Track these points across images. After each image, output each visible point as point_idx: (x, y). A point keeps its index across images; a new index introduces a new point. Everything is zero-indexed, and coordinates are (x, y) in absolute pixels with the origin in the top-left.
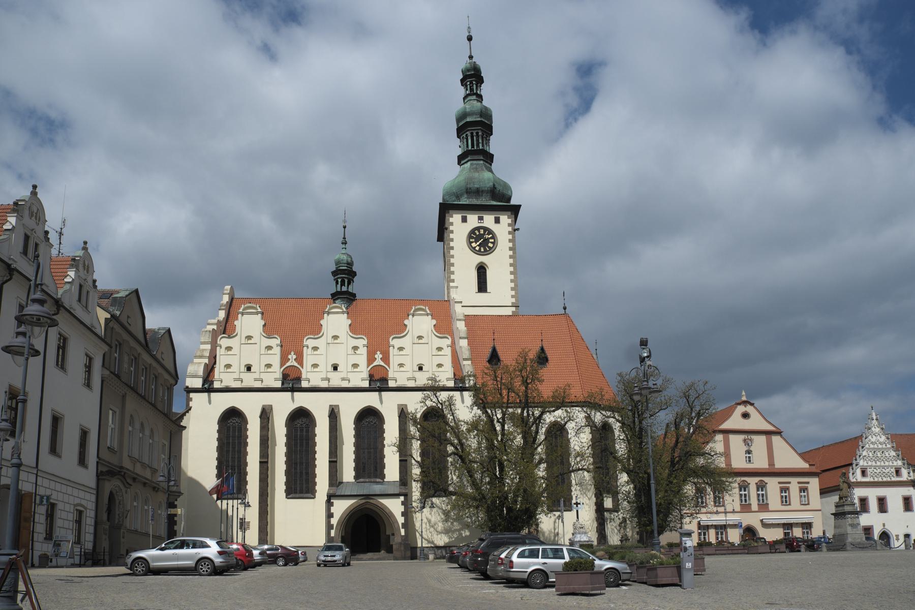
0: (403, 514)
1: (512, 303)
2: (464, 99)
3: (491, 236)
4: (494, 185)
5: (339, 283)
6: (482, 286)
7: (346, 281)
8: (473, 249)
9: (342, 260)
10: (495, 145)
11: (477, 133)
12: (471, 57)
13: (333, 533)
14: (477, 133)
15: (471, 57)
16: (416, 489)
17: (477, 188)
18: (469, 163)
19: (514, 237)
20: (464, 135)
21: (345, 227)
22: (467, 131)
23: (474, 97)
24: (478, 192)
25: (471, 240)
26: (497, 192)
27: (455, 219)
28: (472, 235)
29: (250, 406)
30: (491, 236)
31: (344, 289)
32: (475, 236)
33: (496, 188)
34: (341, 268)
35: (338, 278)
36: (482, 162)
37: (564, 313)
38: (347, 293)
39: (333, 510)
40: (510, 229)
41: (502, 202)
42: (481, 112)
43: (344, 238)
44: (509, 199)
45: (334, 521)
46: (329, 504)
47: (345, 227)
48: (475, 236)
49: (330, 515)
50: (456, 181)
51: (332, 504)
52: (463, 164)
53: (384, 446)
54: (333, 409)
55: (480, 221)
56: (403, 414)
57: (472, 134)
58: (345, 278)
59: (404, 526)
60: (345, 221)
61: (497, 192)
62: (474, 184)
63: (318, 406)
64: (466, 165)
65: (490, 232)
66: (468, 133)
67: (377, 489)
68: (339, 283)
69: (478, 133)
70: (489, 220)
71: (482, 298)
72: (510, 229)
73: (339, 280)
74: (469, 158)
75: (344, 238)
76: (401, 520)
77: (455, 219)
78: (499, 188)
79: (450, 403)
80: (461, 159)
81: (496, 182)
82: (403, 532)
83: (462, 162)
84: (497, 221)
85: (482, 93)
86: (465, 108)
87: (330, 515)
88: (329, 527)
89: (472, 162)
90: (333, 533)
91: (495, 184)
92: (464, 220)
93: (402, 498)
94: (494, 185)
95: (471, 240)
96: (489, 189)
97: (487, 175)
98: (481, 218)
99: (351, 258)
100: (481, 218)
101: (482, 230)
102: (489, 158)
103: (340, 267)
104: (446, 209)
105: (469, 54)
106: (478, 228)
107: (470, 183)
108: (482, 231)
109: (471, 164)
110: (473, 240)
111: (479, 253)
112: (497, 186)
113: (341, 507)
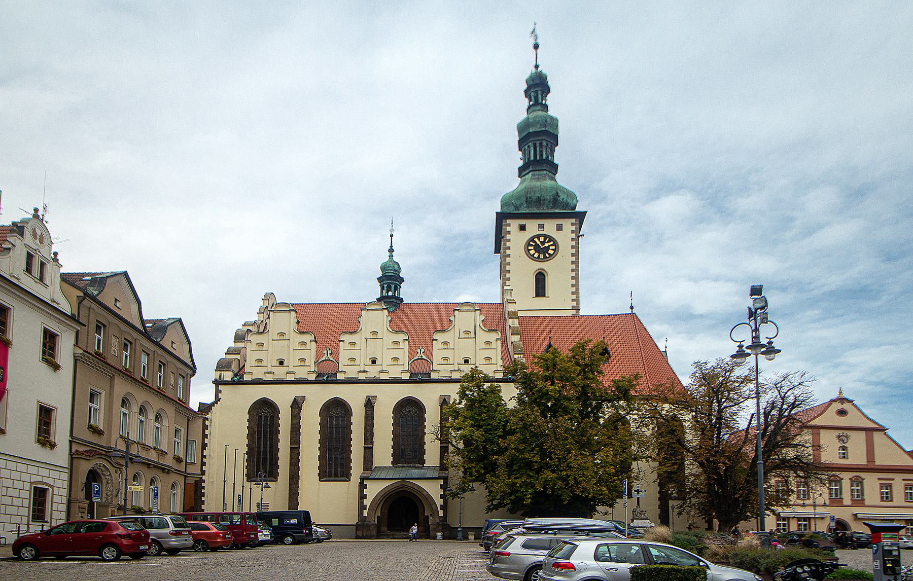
0: (442, 497)
1: (572, 306)
2: (528, 110)
3: (552, 243)
5: (385, 289)
6: (540, 290)
7: (393, 286)
8: (532, 257)
9: (389, 267)
10: (559, 156)
11: (541, 144)
13: (365, 513)
16: (456, 476)
17: (538, 197)
18: (530, 174)
19: (577, 243)
20: (526, 147)
21: (392, 236)
22: (529, 142)
23: (539, 107)
24: (539, 202)
25: (530, 248)
27: (513, 226)
28: (531, 243)
29: (282, 397)
30: (552, 243)
31: (390, 294)
32: (534, 244)
33: (559, 196)
34: (387, 274)
35: (384, 284)
36: (545, 172)
37: (630, 312)
38: (393, 297)
39: (366, 491)
40: (574, 236)
41: (565, 210)
43: (391, 246)
44: (574, 208)
45: (367, 502)
46: (362, 486)
47: (392, 236)
48: (534, 244)
49: (362, 497)
50: (516, 191)
51: (365, 487)
52: (524, 176)
53: (425, 434)
54: (369, 398)
55: (540, 229)
56: (444, 402)
57: (535, 144)
58: (392, 283)
59: (442, 507)
60: (392, 230)
61: (561, 200)
62: (535, 193)
63: (355, 397)
64: (527, 177)
65: (551, 239)
66: (530, 144)
67: (415, 472)
68: (385, 289)
70: (550, 227)
71: (541, 302)
72: (574, 236)
73: (385, 286)
74: (531, 169)
75: (391, 246)
76: (439, 502)
77: (513, 226)
78: (562, 196)
79: (495, 392)
80: (522, 171)
81: (560, 190)
82: (441, 513)
83: (523, 174)
84: (559, 228)
85: (548, 103)
86: (528, 118)
87: (362, 497)
88: (362, 507)
89: (533, 173)
90: (365, 513)
91: (559, 192)
92: (523, 228)
93: (441, 482)
95: (530, 248)
97: (549, 183)
98: (541, 226)
99: (399, 265)
100: (541, 226)
101: (543, 238)
102: (554, 168)
103: (386, 273)
104: (501, 218)
106: (538, 237)
107: (530, 193)
108: (542, 239)
109: (532, 175)
110: (532, 248)
111: (538, 259)
112: (560, 194)
113: (374, 490)
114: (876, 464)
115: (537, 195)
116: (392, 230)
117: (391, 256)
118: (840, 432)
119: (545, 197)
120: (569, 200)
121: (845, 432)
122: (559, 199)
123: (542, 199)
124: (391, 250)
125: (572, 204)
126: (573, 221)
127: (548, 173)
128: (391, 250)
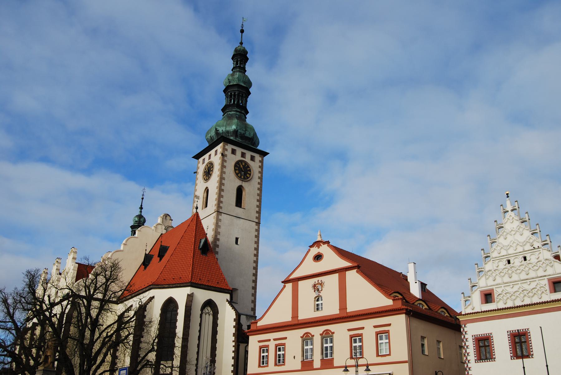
4: (216, 129)
12: (241, 43)
14: (235, 93)
15: (241, 43)
21: (143, 199)
26: (221, 132)
33: (218, 130)
42: (229, 79)
43: (141, 205)
47: (143, 199)
69: (232, 93)
75: (141, 205)
94: (216, 129)
96: (215, 133)
105: (240, 42)
112: (219, 128)
114: (348, 311)
115: (209, 135)
116: (143, 195)
117: (141, 212)
118: (315, 280)
119: (213, 135)
120: (228, 129)
121: (320, 279)
122: (219, 132)
123: (212, 137)
124: (141, 208)
125: (231, 130)
126: (221, 145)
127: (229, 113)
128: (141, 208)
